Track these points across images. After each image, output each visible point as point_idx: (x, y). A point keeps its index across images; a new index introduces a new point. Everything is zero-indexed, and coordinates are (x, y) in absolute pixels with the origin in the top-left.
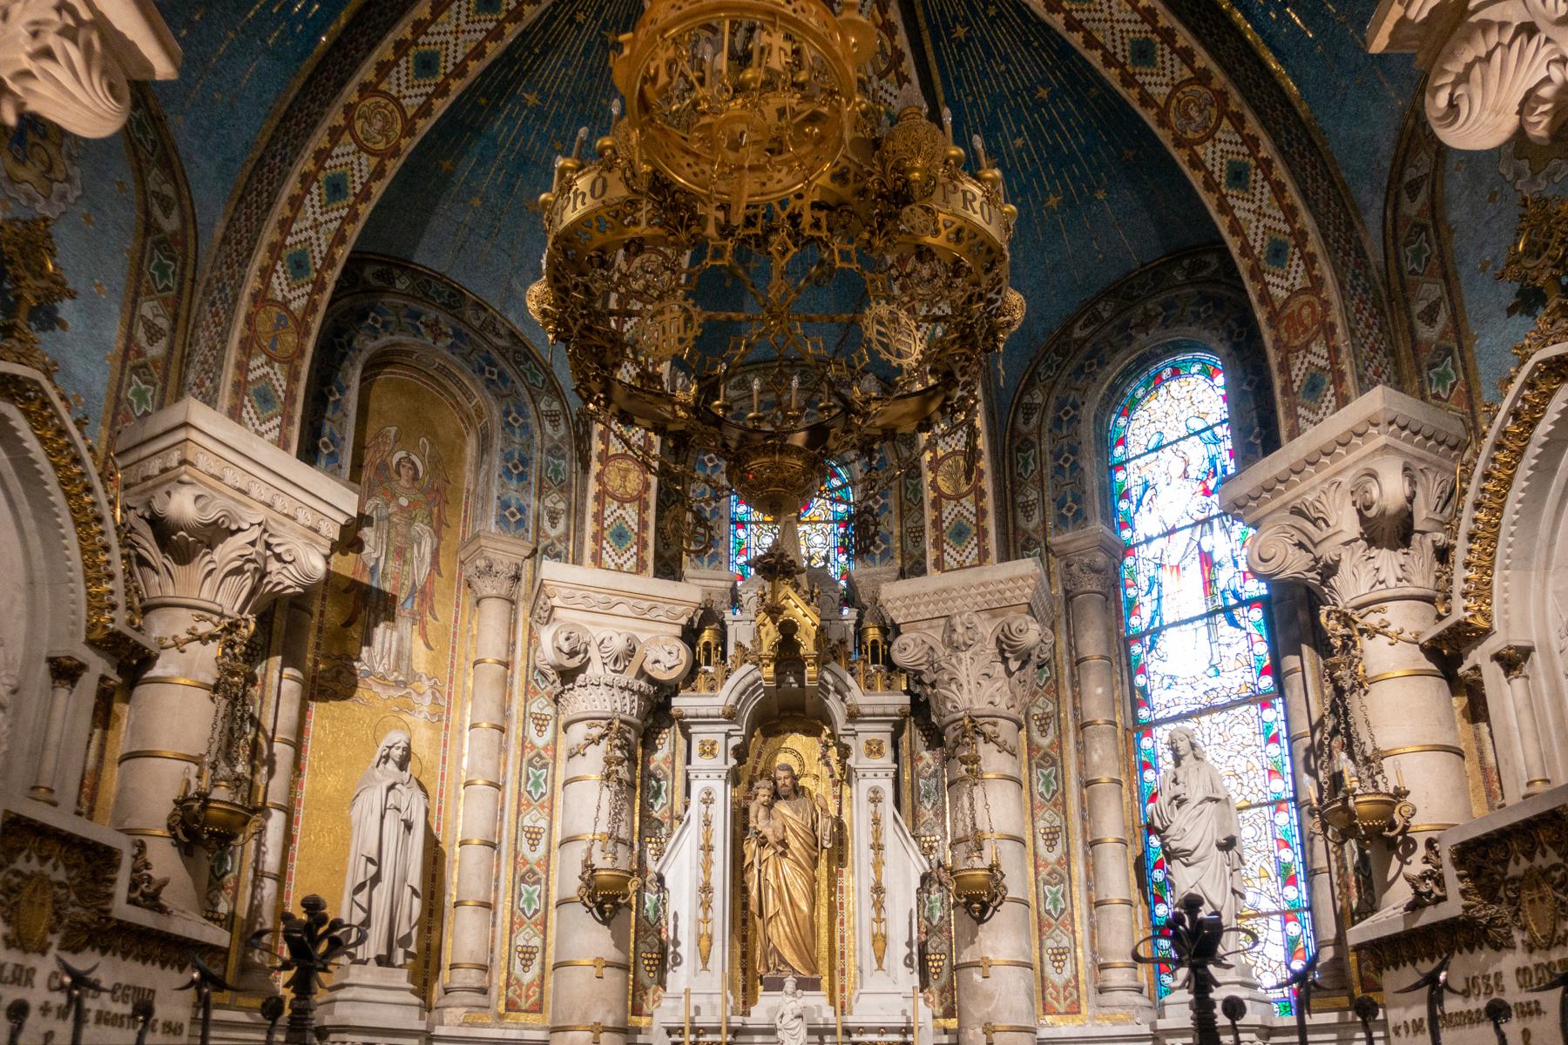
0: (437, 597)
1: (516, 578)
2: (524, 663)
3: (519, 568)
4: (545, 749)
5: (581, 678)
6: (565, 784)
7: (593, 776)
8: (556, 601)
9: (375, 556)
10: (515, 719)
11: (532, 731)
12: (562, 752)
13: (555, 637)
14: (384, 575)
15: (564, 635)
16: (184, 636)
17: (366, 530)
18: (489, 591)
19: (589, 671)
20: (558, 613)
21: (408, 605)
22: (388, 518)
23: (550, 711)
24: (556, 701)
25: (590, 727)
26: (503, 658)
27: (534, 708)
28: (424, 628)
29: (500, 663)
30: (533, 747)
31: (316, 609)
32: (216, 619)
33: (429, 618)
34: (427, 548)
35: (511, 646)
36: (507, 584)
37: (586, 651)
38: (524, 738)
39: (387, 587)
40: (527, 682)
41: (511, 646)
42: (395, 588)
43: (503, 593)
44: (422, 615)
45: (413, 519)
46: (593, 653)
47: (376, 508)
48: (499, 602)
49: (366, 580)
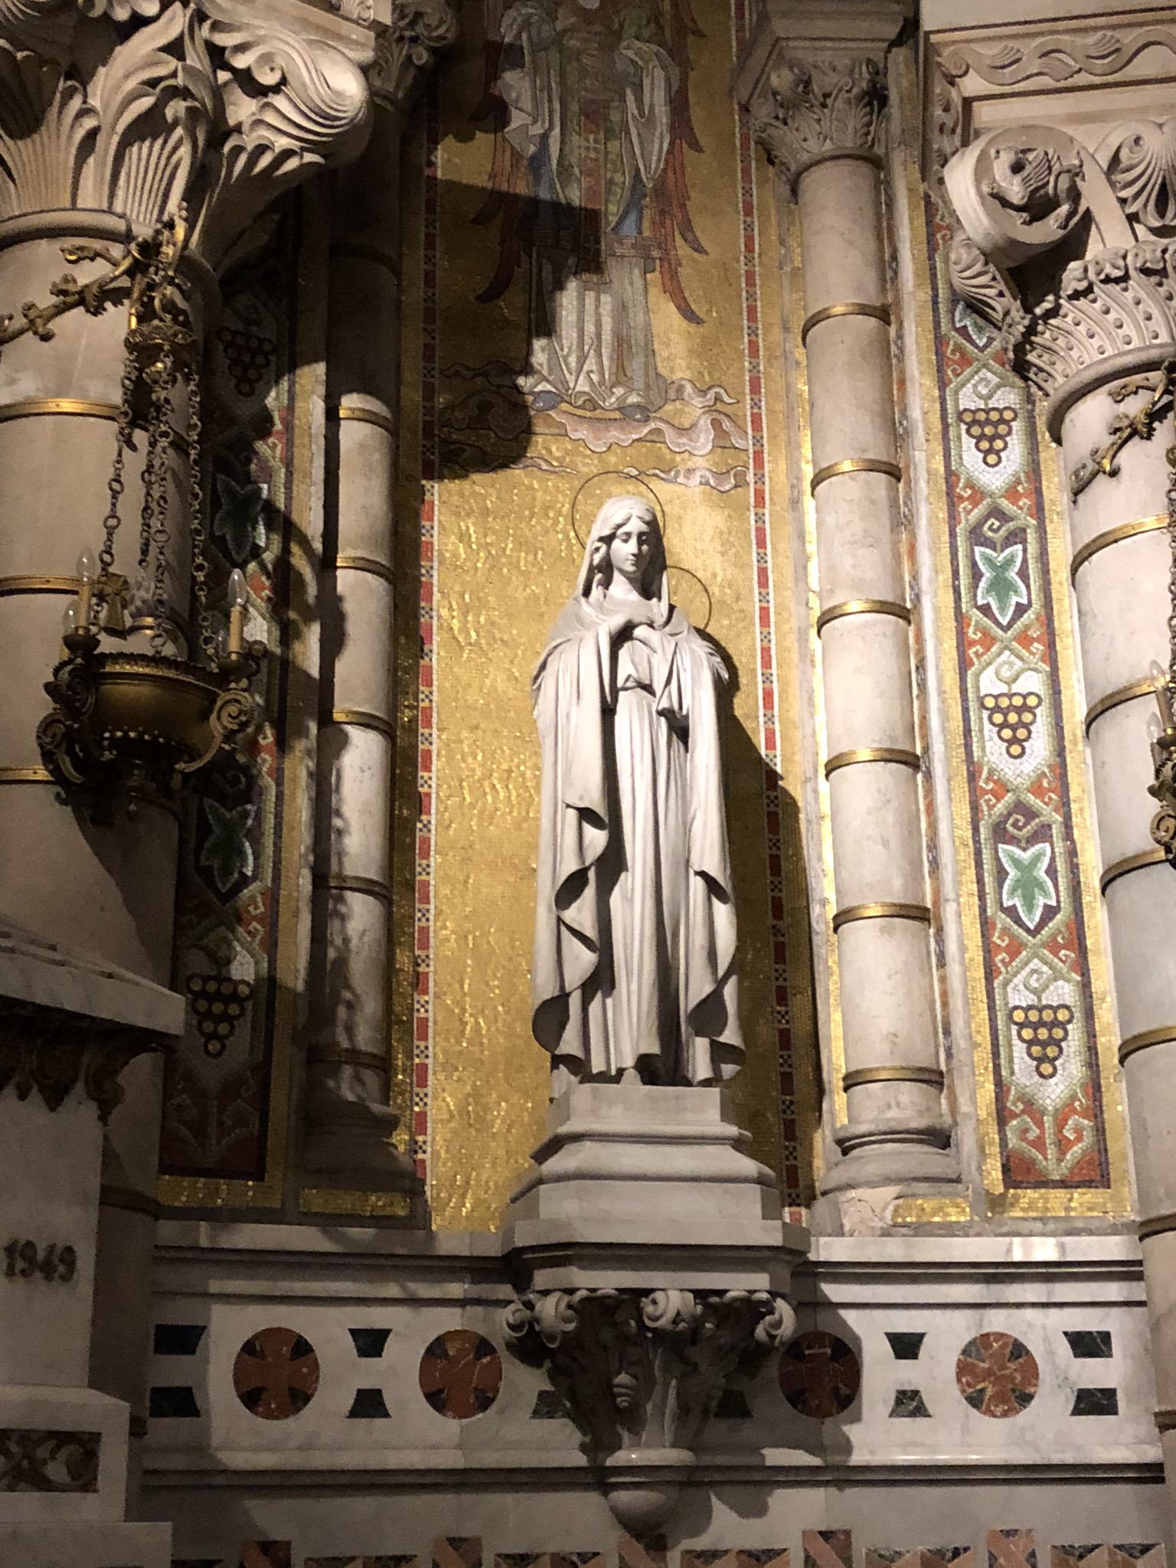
0: (695, 198)
1: (875, 97)
2: (925, 295)
3: (878, 74)
4: (1011, 493)
5: (1072, 275)
6: (1078, 562)
7: (1151, 522)
8: (973, 84)
9: (537, 130)
10: (920, 434)
11: (970, 457)
12: (1056, 489)
13: (982, 170)
14: (564, 168)
15: (1006, 159)
16: (46, 300)
17: (510, 77)
18: (815, 147)
19: (1094, 249)
20: (985, 114)
21: (629, 227)
22: (558, 40)
23: (1008, 398)
24: (1021, 367)
25: (1119, 397)
26: (873, 299)
27: (968, 400)
28: (674, 276)
29: (864, 310)
30: (978, 494)
31: (414, 266)
32: (116, 250)
33: (682, 249)
34: (657, 97)
35: (887, 267)
36: (854, 120)
37: (1075, 195)
38: (951, 476)
39: (575, 195)
40: (940, 341)
41: (887, 267)
42: (592, 193)
43: (849, 141)
44: (665, 246)
45: (618, 35)
46: (1098, 197)
47: (527, 24)
48: (845, 167)
49: (522, 188)
